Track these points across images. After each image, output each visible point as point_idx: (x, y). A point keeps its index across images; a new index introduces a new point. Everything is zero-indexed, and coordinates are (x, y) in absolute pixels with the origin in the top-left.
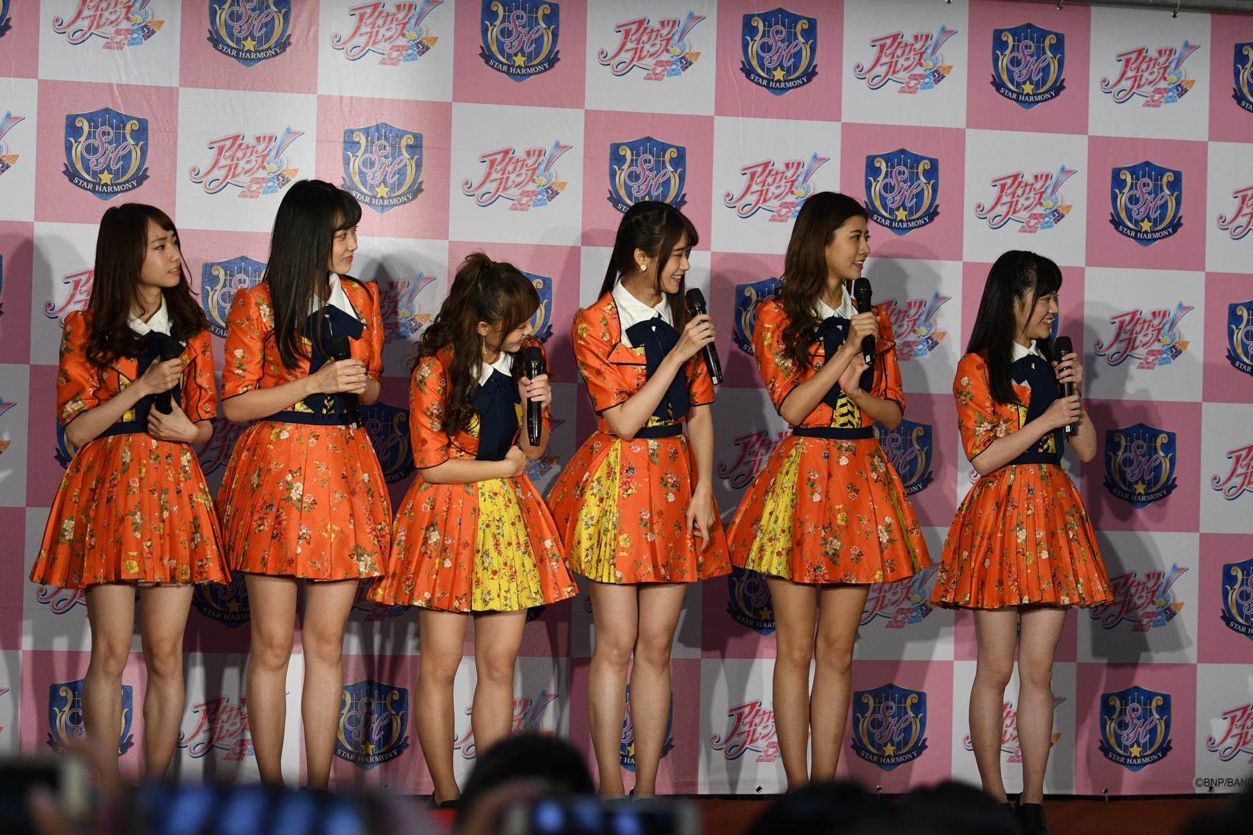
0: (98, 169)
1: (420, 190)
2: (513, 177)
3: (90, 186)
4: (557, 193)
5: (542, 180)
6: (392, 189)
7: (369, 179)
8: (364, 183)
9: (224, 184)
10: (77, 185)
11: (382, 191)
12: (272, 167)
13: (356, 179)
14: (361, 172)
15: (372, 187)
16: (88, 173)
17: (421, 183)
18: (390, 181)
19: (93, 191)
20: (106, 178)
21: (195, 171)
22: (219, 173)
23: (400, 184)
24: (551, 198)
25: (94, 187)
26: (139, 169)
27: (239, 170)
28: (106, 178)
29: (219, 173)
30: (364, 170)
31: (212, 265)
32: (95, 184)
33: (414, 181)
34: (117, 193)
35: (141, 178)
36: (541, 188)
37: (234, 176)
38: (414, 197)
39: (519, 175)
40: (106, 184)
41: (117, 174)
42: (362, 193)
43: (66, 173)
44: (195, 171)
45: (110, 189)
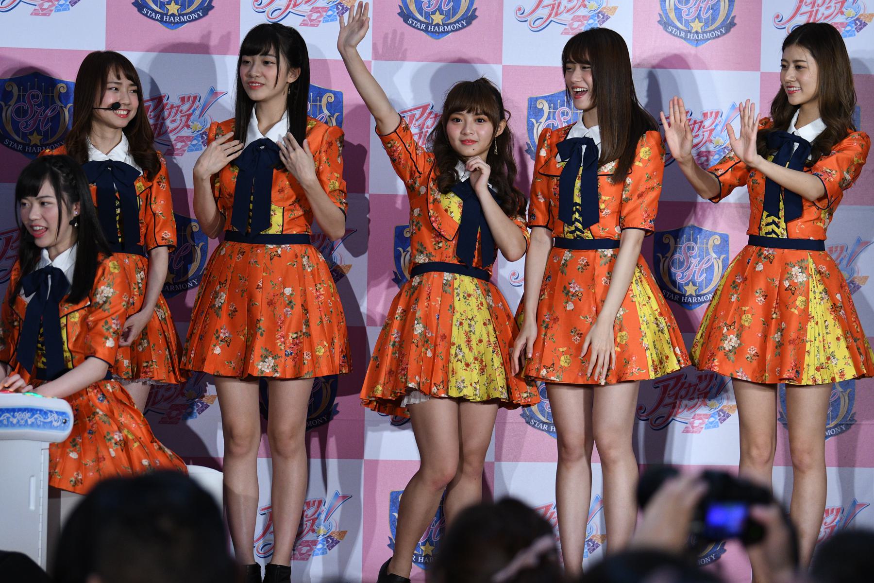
0: (430, 10)
1: (733, 24)
2: (822, 10)
3: (423, 27)
4: (865, 25)
5: (850, 12)
6: (706, 24)
7: (684, 15)
8: (680, 19)
9: (547, 22)
10: (411, 25)
11: (697, 26)
12: (593, 5)
13: (672, 15)
14: (676, 9)
15: (687, 23)
16: (421, 15)
17: (734, 17)
18: (704, 16)
19: (426, 31)
20: (438, 18)
21: (520, 10)
22: (543, 12)
23: (714, 19)
24: (859, 29)
25: (427, 27)
26: (468, 10)
27: (562, 8)
28: (438, 18)
29: (543, 12)
30: (680, 6)
31: (537, 99)
32: (427, 25)
33: (728, 16)
34: (448, 32)
35: (470, 18)
36: (850, 20)
37: (556, 14)
38: (728, 31)
39: (828, 8)
40: (438, 25)
41: (448, 15)
42: (678, 28)
43: (401, 14)
44: (520, 10)
45: (441, 29)
